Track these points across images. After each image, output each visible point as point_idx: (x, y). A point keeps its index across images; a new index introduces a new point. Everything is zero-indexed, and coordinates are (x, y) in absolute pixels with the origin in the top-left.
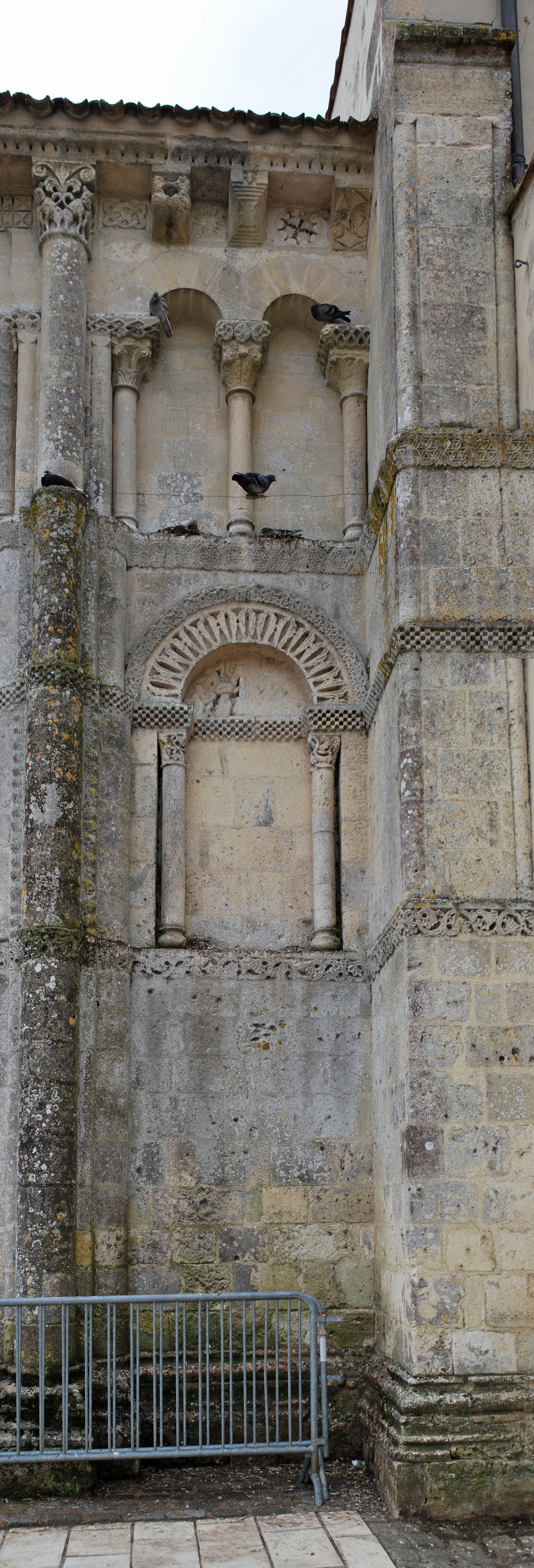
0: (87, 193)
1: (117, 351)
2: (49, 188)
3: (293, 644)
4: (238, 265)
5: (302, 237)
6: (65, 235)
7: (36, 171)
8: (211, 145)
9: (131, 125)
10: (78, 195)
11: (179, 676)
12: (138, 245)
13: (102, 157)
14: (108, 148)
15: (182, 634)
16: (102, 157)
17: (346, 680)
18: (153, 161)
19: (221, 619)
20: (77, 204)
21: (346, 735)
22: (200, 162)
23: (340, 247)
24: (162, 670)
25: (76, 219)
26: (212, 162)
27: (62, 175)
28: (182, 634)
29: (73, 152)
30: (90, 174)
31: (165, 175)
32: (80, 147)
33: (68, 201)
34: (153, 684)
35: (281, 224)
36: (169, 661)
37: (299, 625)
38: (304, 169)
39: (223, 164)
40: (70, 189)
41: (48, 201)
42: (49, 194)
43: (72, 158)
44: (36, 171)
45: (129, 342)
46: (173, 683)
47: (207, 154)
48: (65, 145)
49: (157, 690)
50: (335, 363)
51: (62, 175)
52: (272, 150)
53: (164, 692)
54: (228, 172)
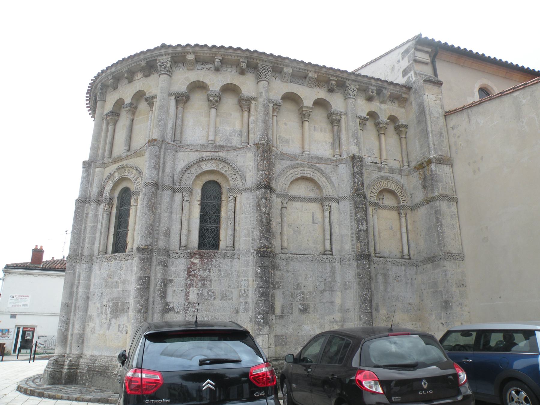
0: (357, 90)
1: (360, 122)
2: (350, 88)
3: (396, 190)
4: (382, 107)
5: (393, 103)
6: (353, 98)
7: (347, 84)
8: (380, 85)
9: (366, 79)
10: (355, 91)
11: (375, 195)
12: (363, 100)
13: (360, 84)
14: (361, 82)
15: (375, 185)
16: (360, 84)
17: (407, 199)
18: (369, 86)
19: (382, 182)
20: (355, 92)
21: (408, 211)
22: (378, 88)
23: (400, 106)
24: (372, 193)
25: (354, 95)
26: (380, 88)
27: (352, 86)
28: (375, 185)
29: (354, 82)
30: (358, 87)
31: (372, 89)
32: (356, 81)
33: (353, 91)
34: (370, 196)
35: (389, 100)
36: (373, 191)
37: (397, 186)
38: (396, 92)
39: (382, 89)
40: (354, 89)
41: (349, 91)
42: (350, 89)
43: (354, 83)
44: (347, 84)
45: (363, 121)
46: (374, 196)
47: (379, 87)
48: (353, 80)
49: (371, 198)
50: (401, 131)
51: (352, 86)
52: (392, 88)
53: (373, 198)
54: (383, 90)
